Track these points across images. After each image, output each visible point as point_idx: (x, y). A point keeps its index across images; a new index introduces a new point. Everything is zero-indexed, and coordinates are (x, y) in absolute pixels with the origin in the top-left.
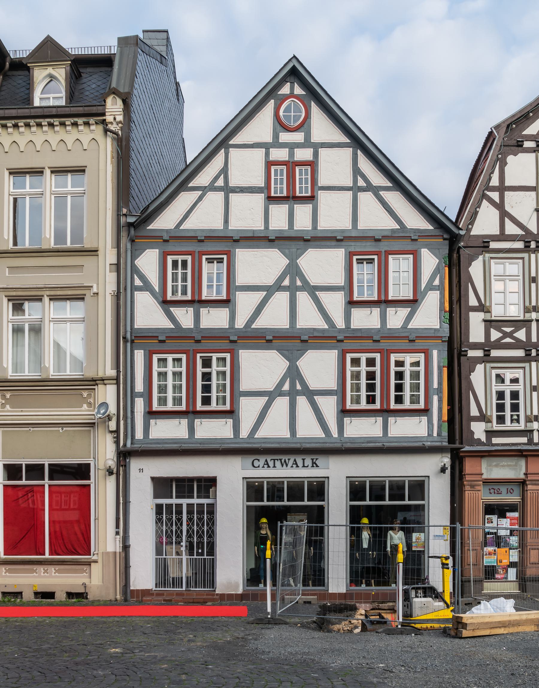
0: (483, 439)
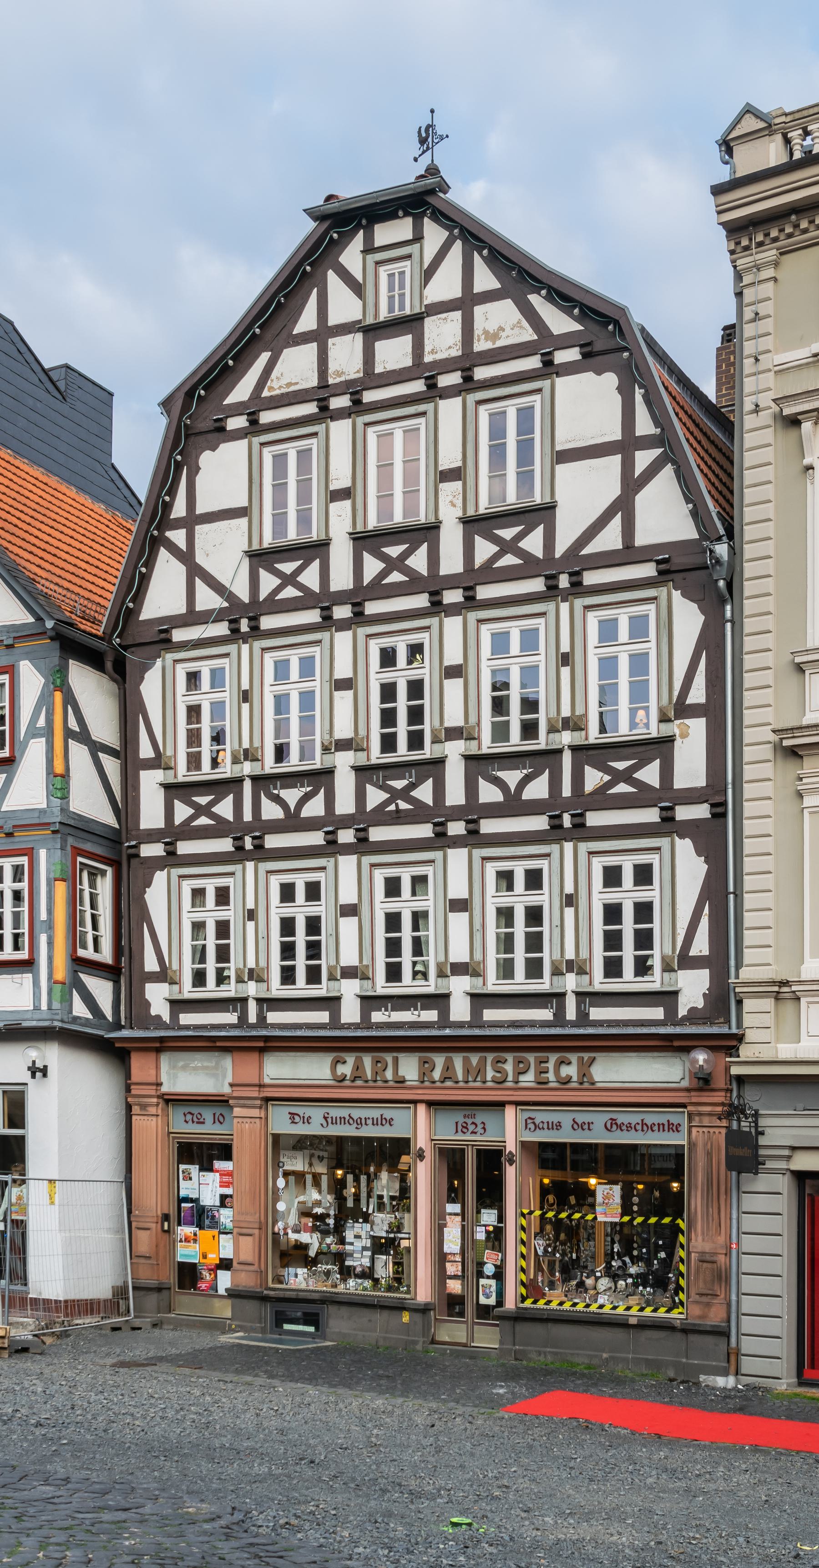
0: (166, 1018)
